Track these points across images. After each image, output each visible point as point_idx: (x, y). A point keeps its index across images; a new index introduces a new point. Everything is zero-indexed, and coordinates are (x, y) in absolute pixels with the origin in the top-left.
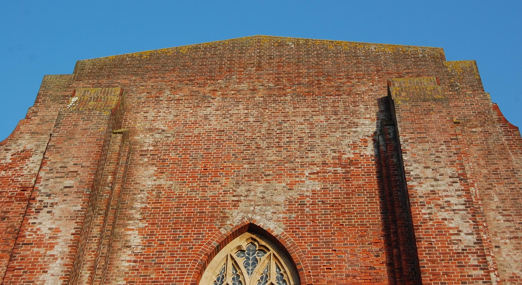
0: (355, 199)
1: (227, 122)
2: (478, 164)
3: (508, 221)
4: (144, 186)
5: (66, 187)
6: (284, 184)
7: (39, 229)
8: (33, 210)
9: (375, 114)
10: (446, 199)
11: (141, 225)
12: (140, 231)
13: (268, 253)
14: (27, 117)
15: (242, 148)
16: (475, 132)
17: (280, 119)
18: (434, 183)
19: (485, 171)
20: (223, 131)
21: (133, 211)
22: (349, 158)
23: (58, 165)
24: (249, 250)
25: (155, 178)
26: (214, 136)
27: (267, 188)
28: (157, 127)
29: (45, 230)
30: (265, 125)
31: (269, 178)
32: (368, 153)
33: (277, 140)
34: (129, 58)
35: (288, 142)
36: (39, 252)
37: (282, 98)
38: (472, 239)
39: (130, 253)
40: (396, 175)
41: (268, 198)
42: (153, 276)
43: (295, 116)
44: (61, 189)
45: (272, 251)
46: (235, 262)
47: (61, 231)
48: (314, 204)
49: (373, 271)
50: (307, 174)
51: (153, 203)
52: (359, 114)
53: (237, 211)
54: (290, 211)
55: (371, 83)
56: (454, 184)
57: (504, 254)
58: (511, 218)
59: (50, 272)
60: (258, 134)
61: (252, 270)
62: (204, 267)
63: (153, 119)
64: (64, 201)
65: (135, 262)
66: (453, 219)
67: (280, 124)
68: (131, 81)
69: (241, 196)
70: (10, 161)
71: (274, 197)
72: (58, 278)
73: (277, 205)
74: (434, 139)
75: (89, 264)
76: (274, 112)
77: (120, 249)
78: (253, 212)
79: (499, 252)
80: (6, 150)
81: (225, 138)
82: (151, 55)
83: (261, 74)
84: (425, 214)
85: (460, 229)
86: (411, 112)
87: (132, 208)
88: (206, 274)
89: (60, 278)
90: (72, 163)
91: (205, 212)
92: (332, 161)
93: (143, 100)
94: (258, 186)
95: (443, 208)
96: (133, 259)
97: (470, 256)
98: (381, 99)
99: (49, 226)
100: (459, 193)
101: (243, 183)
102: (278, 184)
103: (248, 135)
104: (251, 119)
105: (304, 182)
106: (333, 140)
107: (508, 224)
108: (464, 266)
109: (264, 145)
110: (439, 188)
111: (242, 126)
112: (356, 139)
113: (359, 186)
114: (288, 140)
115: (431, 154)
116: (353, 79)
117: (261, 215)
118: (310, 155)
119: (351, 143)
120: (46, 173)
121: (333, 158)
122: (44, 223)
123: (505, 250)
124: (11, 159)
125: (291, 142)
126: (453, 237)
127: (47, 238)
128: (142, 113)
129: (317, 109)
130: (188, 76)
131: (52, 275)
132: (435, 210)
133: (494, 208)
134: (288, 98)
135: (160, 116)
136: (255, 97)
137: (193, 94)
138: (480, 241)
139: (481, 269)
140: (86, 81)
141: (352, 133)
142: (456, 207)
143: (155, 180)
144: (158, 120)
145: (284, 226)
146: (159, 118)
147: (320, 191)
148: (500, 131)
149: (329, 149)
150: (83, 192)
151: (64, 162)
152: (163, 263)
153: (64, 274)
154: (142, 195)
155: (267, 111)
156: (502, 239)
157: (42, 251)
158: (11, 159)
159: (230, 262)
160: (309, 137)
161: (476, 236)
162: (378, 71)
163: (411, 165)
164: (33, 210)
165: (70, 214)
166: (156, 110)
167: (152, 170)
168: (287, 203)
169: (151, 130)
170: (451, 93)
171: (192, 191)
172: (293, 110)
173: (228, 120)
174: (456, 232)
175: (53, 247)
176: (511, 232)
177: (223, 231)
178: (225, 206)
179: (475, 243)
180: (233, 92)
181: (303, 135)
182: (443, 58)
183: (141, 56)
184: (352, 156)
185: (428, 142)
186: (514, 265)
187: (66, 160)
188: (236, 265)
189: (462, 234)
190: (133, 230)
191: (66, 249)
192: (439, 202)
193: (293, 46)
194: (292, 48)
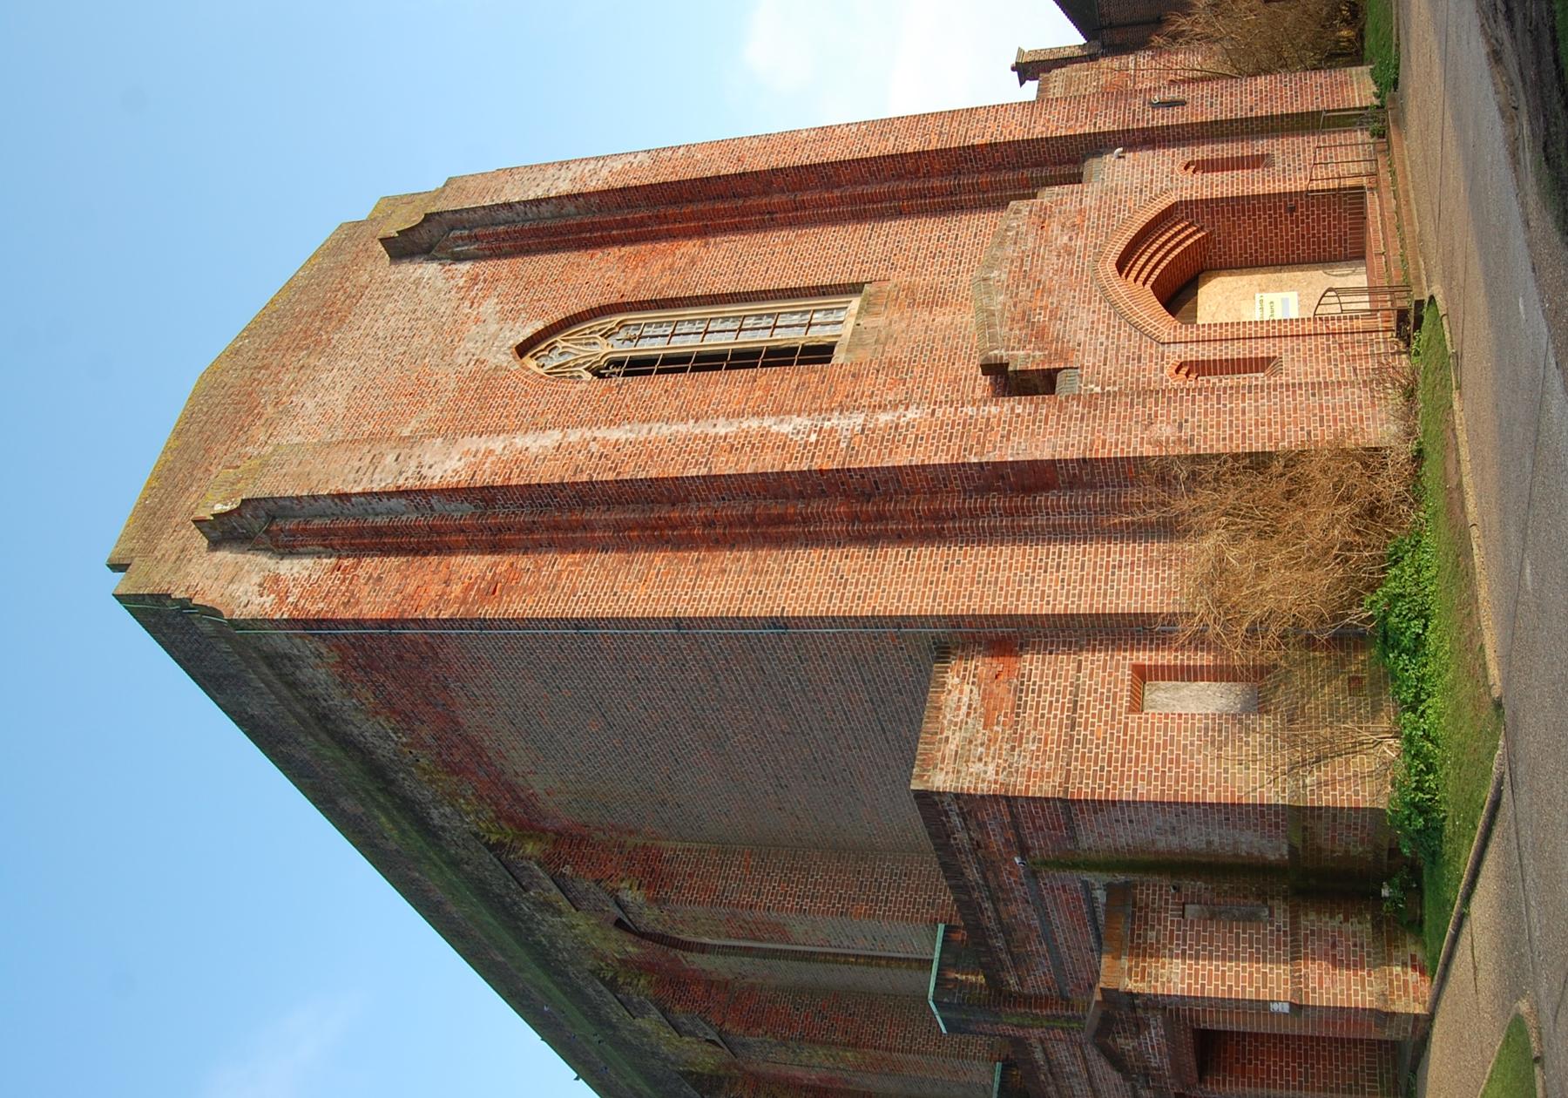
5: (397, 460)
10: (586, 171)
18: (561, 180)
37: (334, 342)
45: (558, 338)
60: (382, 356)
81: (369, 383)
124: (268, 596)
127: (473, 459)
132: (595, 177)
192: (588, 175)
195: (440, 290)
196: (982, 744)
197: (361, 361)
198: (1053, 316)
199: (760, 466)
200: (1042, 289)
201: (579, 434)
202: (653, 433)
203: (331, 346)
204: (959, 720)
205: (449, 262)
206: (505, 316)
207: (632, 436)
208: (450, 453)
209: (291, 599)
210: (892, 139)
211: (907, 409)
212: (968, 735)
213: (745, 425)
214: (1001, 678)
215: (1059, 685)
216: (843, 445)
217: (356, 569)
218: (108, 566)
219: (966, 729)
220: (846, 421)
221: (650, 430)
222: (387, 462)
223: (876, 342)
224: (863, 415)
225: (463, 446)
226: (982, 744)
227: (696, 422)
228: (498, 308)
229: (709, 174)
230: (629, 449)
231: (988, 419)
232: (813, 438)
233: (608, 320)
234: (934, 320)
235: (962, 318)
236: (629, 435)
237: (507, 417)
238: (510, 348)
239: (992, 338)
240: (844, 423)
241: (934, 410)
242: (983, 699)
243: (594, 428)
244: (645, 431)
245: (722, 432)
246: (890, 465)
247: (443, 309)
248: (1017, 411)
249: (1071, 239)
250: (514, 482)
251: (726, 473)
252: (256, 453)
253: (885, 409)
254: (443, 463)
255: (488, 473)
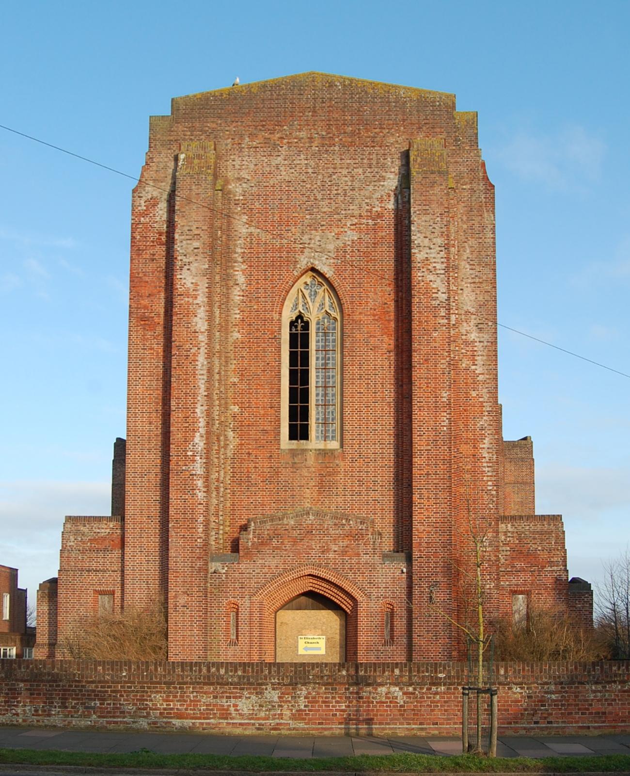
0: (379, 249)
1: (293, 173)
2: (462, 220)
3: (472, 269)
4: (240, 233)
6: (333, 234)
7: (185, 283)
8: (178, 268)
9: (397, 168)
11: (244, 267)
12: (243, 271)
13: (323, 288)
14: (147, 164)
15: (305, 199)
16: (465, 189)
17: (331, 171)
19: (465, 226)
20: (291, 182)
21: (236, 255)
22: (377, 211)
23: (187, 228)
24: (312, 284)
25: (247, 226)
26: (284, 186)
27: (322, 237)
28: (243, 176)
29: (189, 285)
30: (320, 177)
31: (324, 228)
32: (390, 208)
33: (328, 192)
34: (212, 96)
35: (336, 194)
36: (188, 302)
37: (332, 148)
38: (445, 296)
39: (239, 289)
40: (406, 236)
41: (323, 246)
42: (255, 307)
43: (341, 168)
44: (192, 251)
45: (326, 286)
46: (303, 294)
47: (198, 285)
48: (353, 251)
49: (386, 306)
50: (349, 226)
51: (249, 248)
52: (387, 167)
53: (303, 257)
54: (337, 258)
55: (398, 135)
56: (441, 253)
57: (465, 295)
58: (474, 267)
59: (199, 316)
60: (315, 186)
61: (314, 299)
62: (284, 299)
63: (239, 167)
64: (196, 260)
65: (243, 296)
66: (435, 281)
67: (330, 176)
68: (217, 124)
69: (305, 243)
70: (145, 208)
71: (327, 245)
72: (204, 320)
73: (329, 252)
74: (434, 212)
75: (218, 304)
76: (326, 164)
77: (232, 286)
78: (314, 258)
79: (462, 294)
80: (139, 197)
81: (292, 189)
82: (229, 95)
83: (316, 121)
84: (419, 277)
85: (439, 289)
86: (422, 184)
87: (236, 253)
88: (286, 303)
89: (206, 321)
90: (195, 227)
91: (283, 257)
92: (365, 214)
93: (229, 147)
94: (316, 235)
95: (431, 272)
96: (242, 294)
97: (441, 309)
98: (403, 152)
99: (191, 281)
100: (442, 260)
101: (306, 232)
102: (329, 234)
103: (308, 186)
104: (310, 171)
105: (346, 232)
106: (367, 194)
107: (471, 272)
108: (437, 316)
109: (319, 197)
110: (431, 255)
111: (303, 178)
112: (383, 193)
113: (382, 238)
114: (336, 192)
115: (430, 226)
116: (384, 129)
117: (319, 260)
118: (351, 207)
119: (380, 197)
120: (180, 235)
121: (366, 212)
122: (187, 278)
123: (466, 291)
124: (145, 206)
125: (339, 194)
126: (434, 295)
127: (192, 290)
128: (231, 161)
129: (357, 161)
130: (261, 121)
131: (201, 318)
133: (465, 258)
134: (337, 148)
135: (244, 165)
136: (312, 146)
137: (267, 141)
138: (448, 299)
139: (446, 319)
140: (183, 124)
141: (380, 187)
142: (438, 272)
143: (247, 228)
144: (243, 169)
145: (333, 270)
146: (243, 167)
147: (357, 241)
148: (482, 189)
149: (364, 202)
150: (206, 253)
151: (189, 226)
152: (260, 298)
153: (207, 318)
154: (241, 242)
155: (321, 161)
156: (466, 283)
157: (191, 300)
158: (145, 206)
159: (300, 294)
160: (351, 190)
161: (447, 294)
162: (404, 120)
163: (416, 235)
164: (178, 268)
165: (202, 271)
166: (240, 159)
167: (245, 218)
168: (335, 251)
169: (238, 179)
170: (454, 148)
171: (273, 238)
172: (340, 162)
173: (293, 171)
174: (436, 291)
175: (196, 297)
176: (472, 278)
177: (296, 274)
178: (295, 252)
179: (446, 300)
180: (296, 140)
181: (347, 188)
182: (454, 107)
183: (222, 95)
184: (379, 209)
185: (429, 214)
186: (469, 304)
187: (190, 224)
188: (304, 296)
189: (440, 293)
190: (238, 271)
191: (205, 299)
193: (340, 87)
194: (339, 89)
195: (370, 198)
196: (82, 539)
197: (312, 175)
198: (277, 548)
199: (174, 433)
200: (295, 541)
201: (203, 340)
202: (200, 377)
203: (328, 148)
204: (94, 529)
205: (397, 192)
206: (341, 252)
207: (199, 367)
208: (197, 276)
209: (142, 219)
210: (429, 448)
211: (204, 492)
212: (86, 534)
213: (200, 420)
214: (112, 542)
215: (107, 564)
216: (184, 468)
217: (158, 245)
218: (173, 100)
219: (88, 533)
220: (199, 467)
221: (203, 375)
222: (194, 244)
223: (295, 463)
224: (202, 473)
225: (201, 281)
226: (82, 539)
227: (205, 396)
228: (349, 243)
229: (415, 346)
230: (190, 369)
231: (195, 528)
232: (190, 453)
233: (338, 311)
234: (308, 488)
235: (308, 502)
236: (200, 365)
237: (258, 283)
238: (312, 264)
239: (265, 522)
240: (198, 465)
241: (202, 504)
242: (102, 537)
243: (206, 346)
244: (202, 372)
245: (197, 410)
246: (170, 490)
247: (351, 207)
248: (199, 540)
249: (335, 551)
250: (174, 318)
251: (172, 419)
252: (243, 146)
253: (204, 482)
254: (191, 275)
255: (182, 302)
